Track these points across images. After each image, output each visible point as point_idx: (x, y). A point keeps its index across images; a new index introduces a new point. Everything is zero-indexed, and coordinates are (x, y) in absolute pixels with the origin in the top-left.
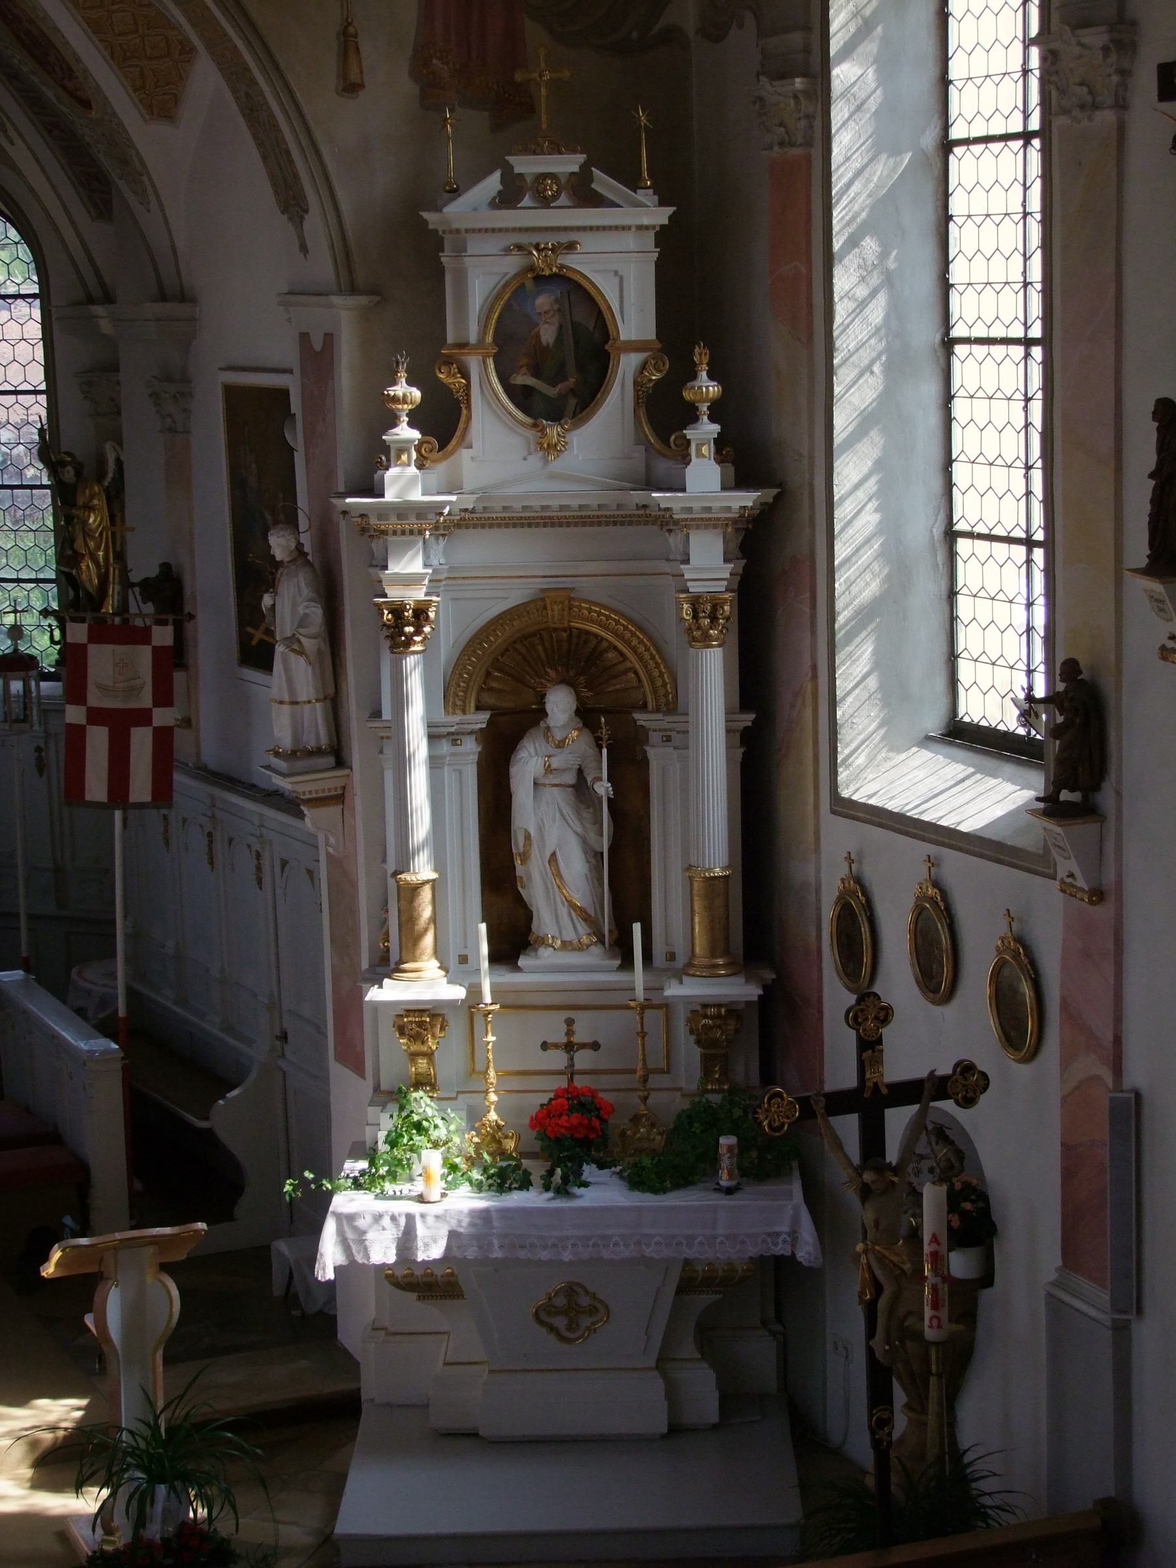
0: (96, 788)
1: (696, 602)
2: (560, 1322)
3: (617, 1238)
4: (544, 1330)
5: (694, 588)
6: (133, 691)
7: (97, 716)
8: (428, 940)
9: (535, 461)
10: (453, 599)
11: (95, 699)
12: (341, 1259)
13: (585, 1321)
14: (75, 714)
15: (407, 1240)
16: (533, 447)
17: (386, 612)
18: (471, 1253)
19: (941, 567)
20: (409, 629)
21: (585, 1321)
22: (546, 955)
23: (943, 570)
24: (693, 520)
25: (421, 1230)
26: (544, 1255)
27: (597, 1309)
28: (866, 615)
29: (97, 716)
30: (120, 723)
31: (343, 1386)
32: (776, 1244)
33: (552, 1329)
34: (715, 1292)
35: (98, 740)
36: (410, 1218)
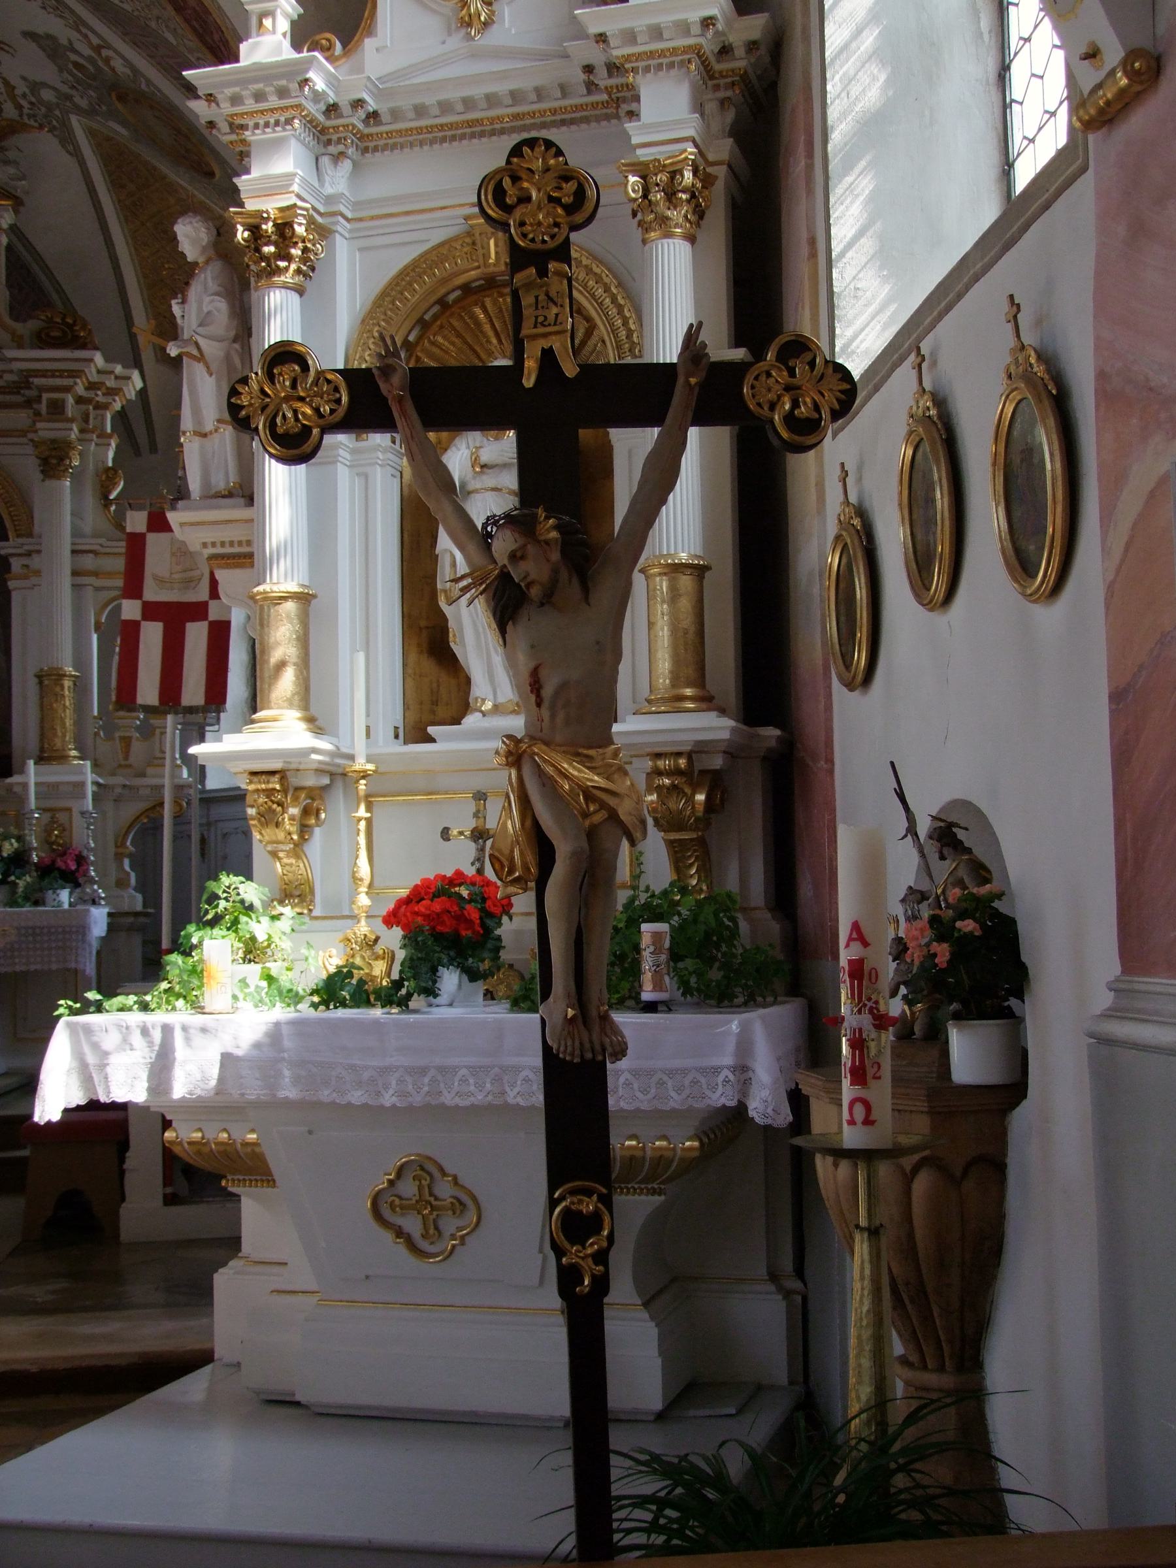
0: (148, 691)
1: (644, 171)
2: (412, 1224)
3: (464, 1071)
4: (388, 1236)
5: (644, 154)
6: (189, 583)
7: (152, 611)
8: (287, 682)
9: (456, 41)
10: (360, 250)
11: (152, 593)
12: (78, 1098)
13: (449, 1224)
14: (131, 610)
15: (161, 1067)
16: (453, 26)
17: (240, 228)
18: (254, 1091)
19: (986, 37)
20: (269, 249)
21: (449, 1224)
22: (471, 721)
23: (989, 39)
24: (639, 56)
25: (180, 1050)
26: (357, 1097)
27: (465, 1203)
28: (874, 127)
29: (152, 611)
30: (176, 618)
31: (206, 1346)
32: (714, 1089)
33: (399, 1233)
34: (654, 1192)
35: (152, 635)
36: (167, 1030)
